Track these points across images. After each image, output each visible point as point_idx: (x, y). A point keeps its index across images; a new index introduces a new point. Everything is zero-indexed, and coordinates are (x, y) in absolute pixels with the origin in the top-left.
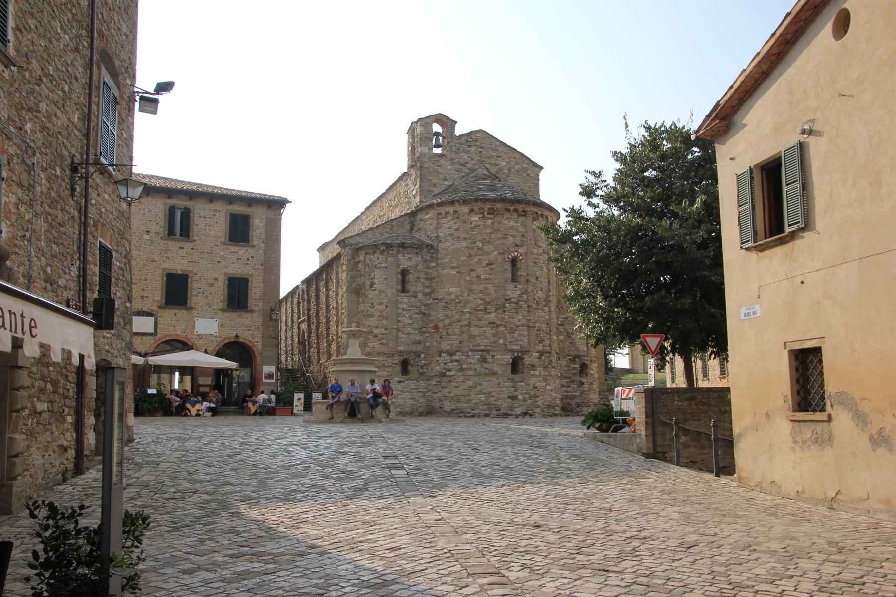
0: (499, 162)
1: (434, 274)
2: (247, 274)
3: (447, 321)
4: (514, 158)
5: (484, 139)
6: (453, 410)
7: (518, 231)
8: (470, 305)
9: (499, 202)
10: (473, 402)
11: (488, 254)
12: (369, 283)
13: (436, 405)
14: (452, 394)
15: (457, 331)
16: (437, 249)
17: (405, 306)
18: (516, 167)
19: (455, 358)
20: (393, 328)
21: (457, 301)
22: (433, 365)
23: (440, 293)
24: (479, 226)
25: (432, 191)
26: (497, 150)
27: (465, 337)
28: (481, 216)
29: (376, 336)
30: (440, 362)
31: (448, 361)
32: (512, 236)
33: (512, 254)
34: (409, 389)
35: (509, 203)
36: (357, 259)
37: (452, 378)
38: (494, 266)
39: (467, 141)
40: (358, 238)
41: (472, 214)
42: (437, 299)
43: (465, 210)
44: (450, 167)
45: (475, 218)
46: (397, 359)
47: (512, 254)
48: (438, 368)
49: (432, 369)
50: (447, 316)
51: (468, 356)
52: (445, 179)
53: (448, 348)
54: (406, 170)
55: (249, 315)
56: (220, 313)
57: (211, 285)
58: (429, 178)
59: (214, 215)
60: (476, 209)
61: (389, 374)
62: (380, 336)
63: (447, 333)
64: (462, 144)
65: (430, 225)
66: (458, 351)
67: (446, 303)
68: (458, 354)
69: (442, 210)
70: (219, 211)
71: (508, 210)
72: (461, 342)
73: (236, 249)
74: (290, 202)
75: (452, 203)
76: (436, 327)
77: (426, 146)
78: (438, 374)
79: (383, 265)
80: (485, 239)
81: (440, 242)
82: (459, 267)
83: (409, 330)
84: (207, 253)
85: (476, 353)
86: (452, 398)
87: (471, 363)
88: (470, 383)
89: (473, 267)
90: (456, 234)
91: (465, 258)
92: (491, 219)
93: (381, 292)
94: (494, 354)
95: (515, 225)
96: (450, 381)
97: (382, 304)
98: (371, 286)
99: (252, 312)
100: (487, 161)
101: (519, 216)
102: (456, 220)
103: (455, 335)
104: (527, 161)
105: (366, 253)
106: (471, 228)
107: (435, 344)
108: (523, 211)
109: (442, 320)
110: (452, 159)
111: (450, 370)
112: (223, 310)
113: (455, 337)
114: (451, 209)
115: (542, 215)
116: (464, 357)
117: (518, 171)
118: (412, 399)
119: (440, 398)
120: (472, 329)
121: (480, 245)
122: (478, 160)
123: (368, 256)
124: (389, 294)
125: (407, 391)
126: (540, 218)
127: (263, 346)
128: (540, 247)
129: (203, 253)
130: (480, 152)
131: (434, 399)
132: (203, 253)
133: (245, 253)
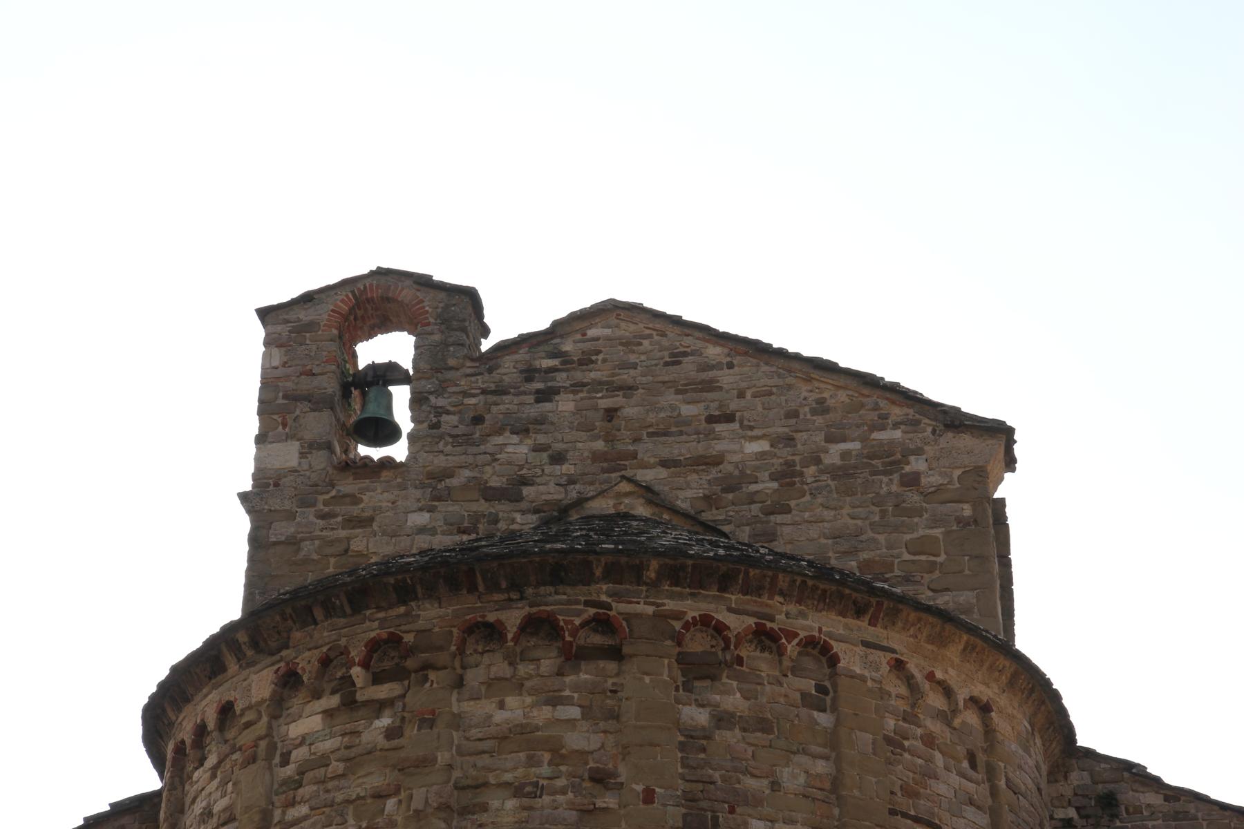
0: (719, 446)
4: (821, 408)
5: (629, 344)
7: (559, 755)
9: (431, 593)
18: (833, 454)
24: (323, 761)
26: (710, 386)
28: (334, 701)
32: (517, 790)
35: (493, 587)
39: (529, 373)
41: (296, 703)
44: (422, 519)
60: (307, 663)
64: (501, 391)
71: (492, 633)
77: (288, 437)
95: (544, 714)
100: (648, 449)
101: (574, 656)
104: (897, 412)
108: (603, 624)
115: (766, 638)
117: (842, 473)
122: (596, 457)
126: (760, 662)
130: (611, 414)
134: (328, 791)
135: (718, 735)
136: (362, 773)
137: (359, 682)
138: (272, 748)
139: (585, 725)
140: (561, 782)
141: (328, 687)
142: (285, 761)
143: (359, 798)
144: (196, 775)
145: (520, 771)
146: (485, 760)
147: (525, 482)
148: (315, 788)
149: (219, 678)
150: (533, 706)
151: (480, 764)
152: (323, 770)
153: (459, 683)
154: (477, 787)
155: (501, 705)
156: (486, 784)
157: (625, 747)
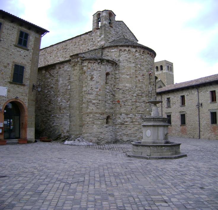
1: (118, 77)
2: (24, 64)
3: (125, 99)
6: (128, 140)
8: (136, 93)
10: (138, 137)
11: (142, 70)
12: (90, 77)
13: (119, 138)
14: (128, 133)
15: (129, 104)
16: (119, 66)
17: (108, 90)
19: (129, 116)
20: (103, 101)
21: (130, 90)
22: (117, 119)
23: (121, 86)
24: (139, 58)
25: (108, 40)
27: (134, 107)
29: (94, 104)
30: (121, 118)
31: (126, 118)
34: (110, 131)
36: (83, 65)
37: (127, 126)
38: (145, 76)
40: (84, 55)
41: (137, 52)
42: (119, 89)
43: (134, 50)
44: (114, 32)
45: (137, 54)
46: (105, 116)
48: (120, 120)
49: (116, 121)
50: (124, 97)
51: (135, 116)
52: (112, 37)
53: (125, 111)
54: (92, 30)
55: (22, 87)
56: (9, 84)
57: (5, 67)
58: (108, 35)
59: (12, 29)
61: (102, 123)
62: (97, 104)
63: (124, 104)
65: (115, 54)
66: (130, 113)
67: (123, 91)
68: (131, 114)
69: (123, 49)
70: (15, 28)
71: (148, 53)
72: (131, 109)
73: (20, 50)
74: (48, 32)
75: (128, 46)
76: (119, 102)
78: (120, 123)
79: (99, 69)
81: (120, 62)
82: (130, 75)
83: (109, 102)
84: (6, 49)
85: (139, 114)
86: (128, 135)
87: (137, 119)
88: (136, 128)
89: (137, 76)
90: (129, 60)
91: (134, 71)
92: (143, 56)
93: (97, 82)
94: (146, 115)
96: (126, 127)
97: (97, 88)
98: (92, 79)
99: (24, 85)
102: (129, 54)
103: (129, 105)
105: (89, 62)
106: (136, 58)
107: (118, 109)
109: (121, 99)
110: (114, 30)
111: (127, 122)
112: (10, 83)
113: (129, 106)
114: (127, 49)
116: (134, 116)
118: (111, 135)
119: (121, 135)
120: (137, 103)
121: (140, 66)
123: (90, 64)
124: (102, 84)
125: (109, 132)
127: (29, 105)
129: (4, 48)
131: (118, 135)
132: (4, 48)
133: (24, 53)
147: (118, 32)
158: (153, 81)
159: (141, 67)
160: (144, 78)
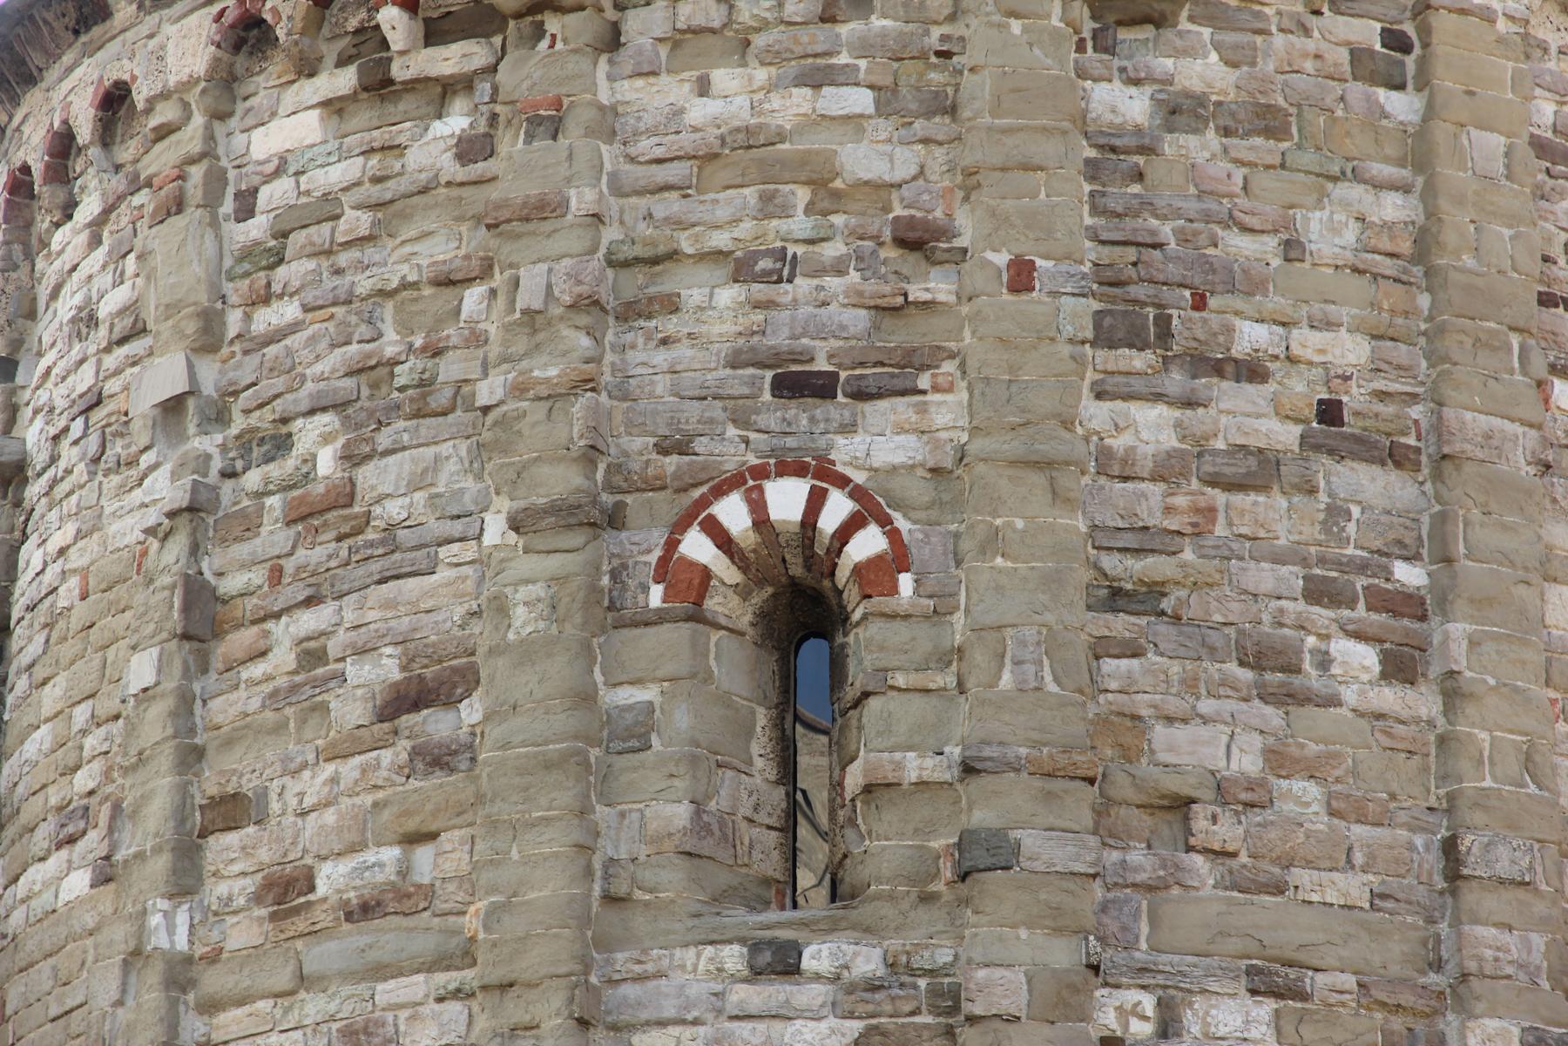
24: (327, 208)
28: (344, 80)
32: (742, 269)
33: (733, 513)
38: (471, 711)
41: (263, 83)
47: (733, 513)
80: (372, 370)
121: (326, 463)
128: (1252, 371)
134: (338, 272)
135: (1171, 145)
136: (410, 232)
137: (397, 41)
138: (216, 181)
139: (884, 127)
140: (833, 250)
141: (330, 52)
142: (246, 207)
143: (405, 285)
144: (58, 238)
145: (746, 229)
146: (671, 205)
148: (311, 265)
149: (96, 31)
150: (770, 88)
151: (660, 212)
152: (326, 227)
153: (613, 41)
154: (655, 261)
155: (703, 88)
156: (673, 255)
157: (969, 173)
158: (915, 766)
159: (351, 458)
160: (435, 759)
